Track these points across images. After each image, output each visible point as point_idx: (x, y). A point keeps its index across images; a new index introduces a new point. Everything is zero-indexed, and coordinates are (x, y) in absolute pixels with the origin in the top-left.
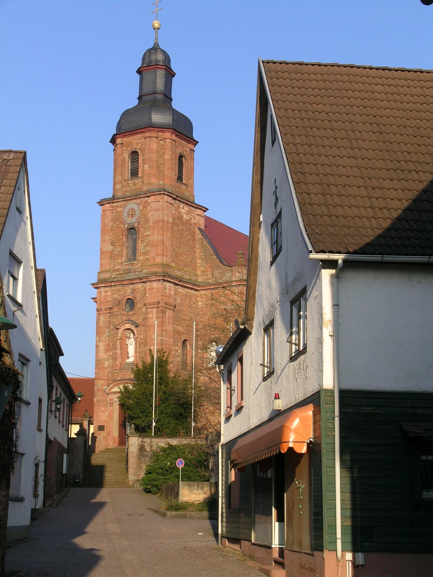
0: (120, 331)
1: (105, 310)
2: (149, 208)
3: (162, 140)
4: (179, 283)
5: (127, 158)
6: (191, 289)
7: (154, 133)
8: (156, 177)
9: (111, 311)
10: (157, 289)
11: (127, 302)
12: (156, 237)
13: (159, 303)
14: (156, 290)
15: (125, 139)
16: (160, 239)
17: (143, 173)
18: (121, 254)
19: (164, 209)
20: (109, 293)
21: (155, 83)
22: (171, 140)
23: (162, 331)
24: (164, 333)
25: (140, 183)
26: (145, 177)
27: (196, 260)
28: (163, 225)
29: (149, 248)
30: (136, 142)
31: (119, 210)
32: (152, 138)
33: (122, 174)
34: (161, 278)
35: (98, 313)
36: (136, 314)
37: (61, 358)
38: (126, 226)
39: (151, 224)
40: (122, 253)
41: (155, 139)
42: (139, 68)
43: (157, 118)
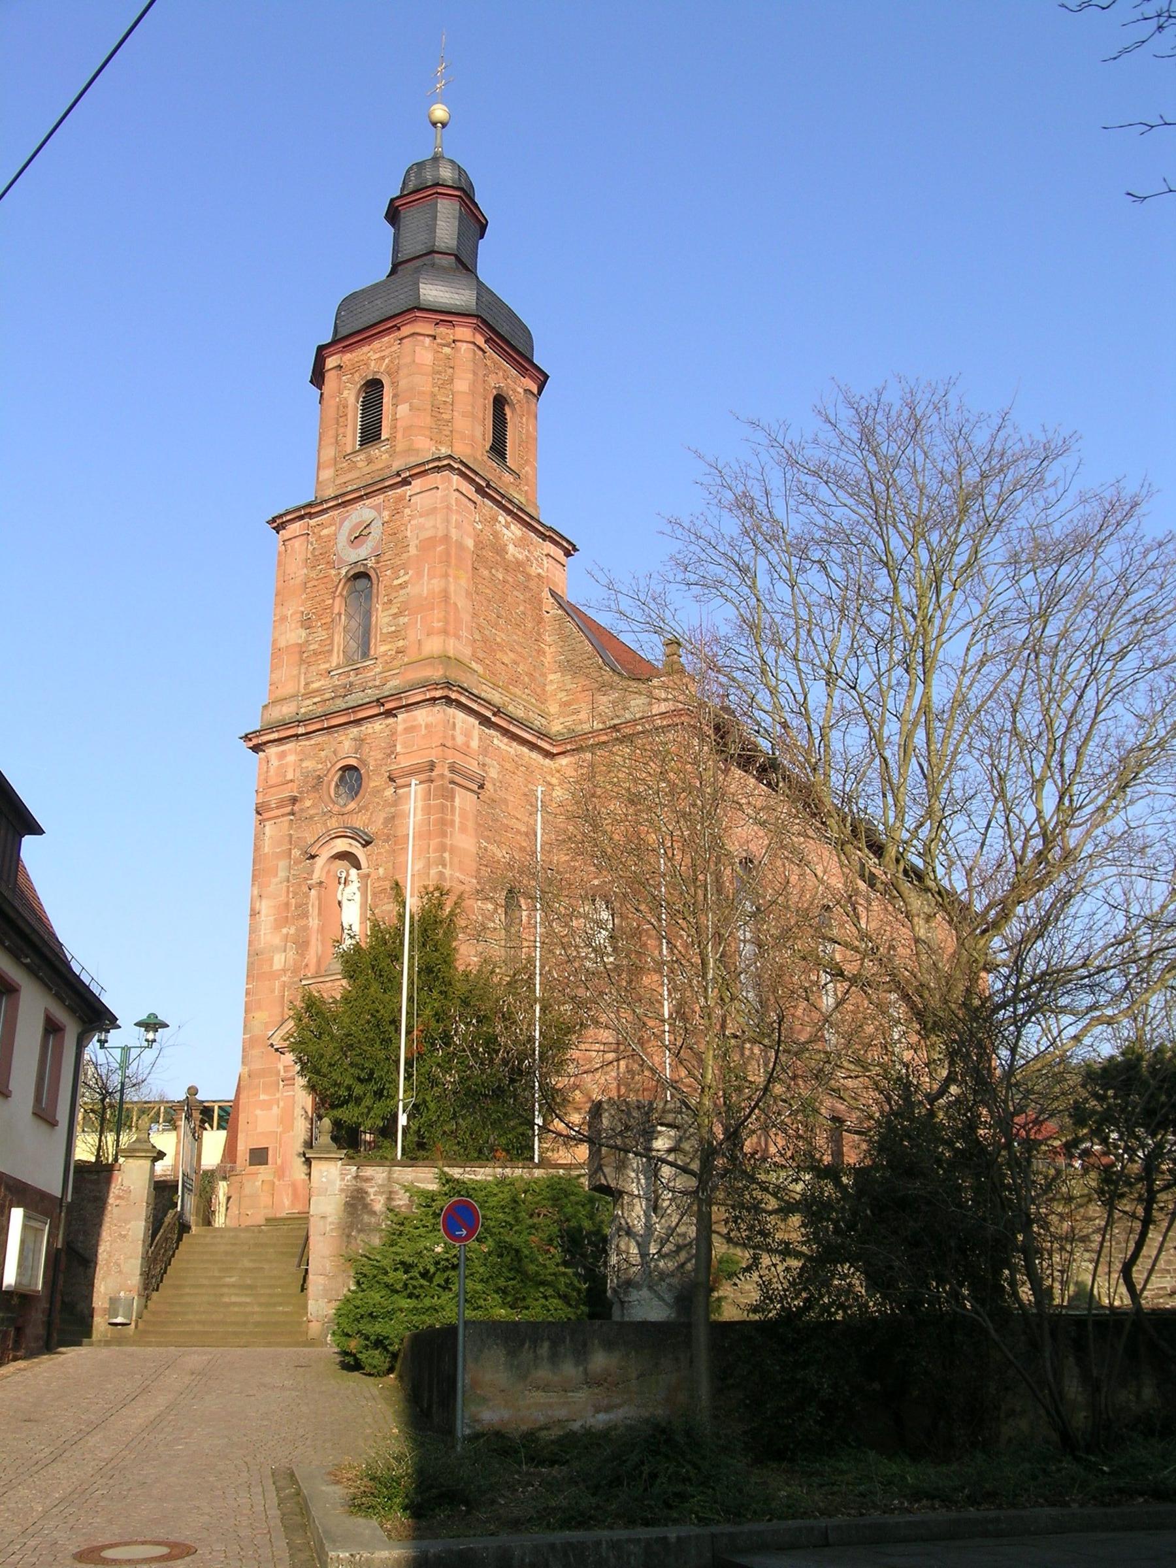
0: (320, 862)
1: (277, 808)
2: (407, 511)
3: (448, 345)
4: (493, 719)
5: (352, 399)
6: (533, 747)
7: (427, 325)
8: (427, 433)
9: (296, 808)
10: (427, 726)
11: (342, 778)
12: (424, 586)
13: (432, 766)
14: (423, 732)
15: (348, 356)
16: (437, 590)
17: (394, 428)
18: (327, 648)
19: (448, 507)
20: (291, 758)
21: (432, 229)
22: (471, 346)
23: (443, 848)
24: (446, 855)
25: (384, 457)
26: (399, 436)
27: (544, 675)
28: (447, 553)
29: (406, 620)
30: (377, 356)
31: (325, 532)
32: (421, 338)
33: (337, 442)
34: (438, 694)
35: (260, 817)
36: (366, 808)
37: (29, 843)
38: (343, 571)
39: (413, 550)
40: (332, 644)
41: (428, 340)
42: (392, 200)
43: (433, 292)
